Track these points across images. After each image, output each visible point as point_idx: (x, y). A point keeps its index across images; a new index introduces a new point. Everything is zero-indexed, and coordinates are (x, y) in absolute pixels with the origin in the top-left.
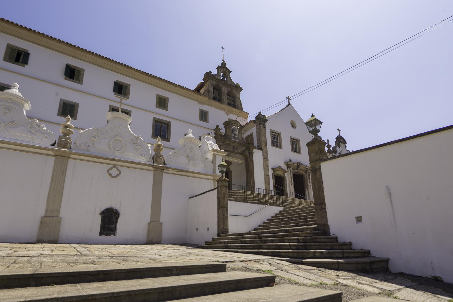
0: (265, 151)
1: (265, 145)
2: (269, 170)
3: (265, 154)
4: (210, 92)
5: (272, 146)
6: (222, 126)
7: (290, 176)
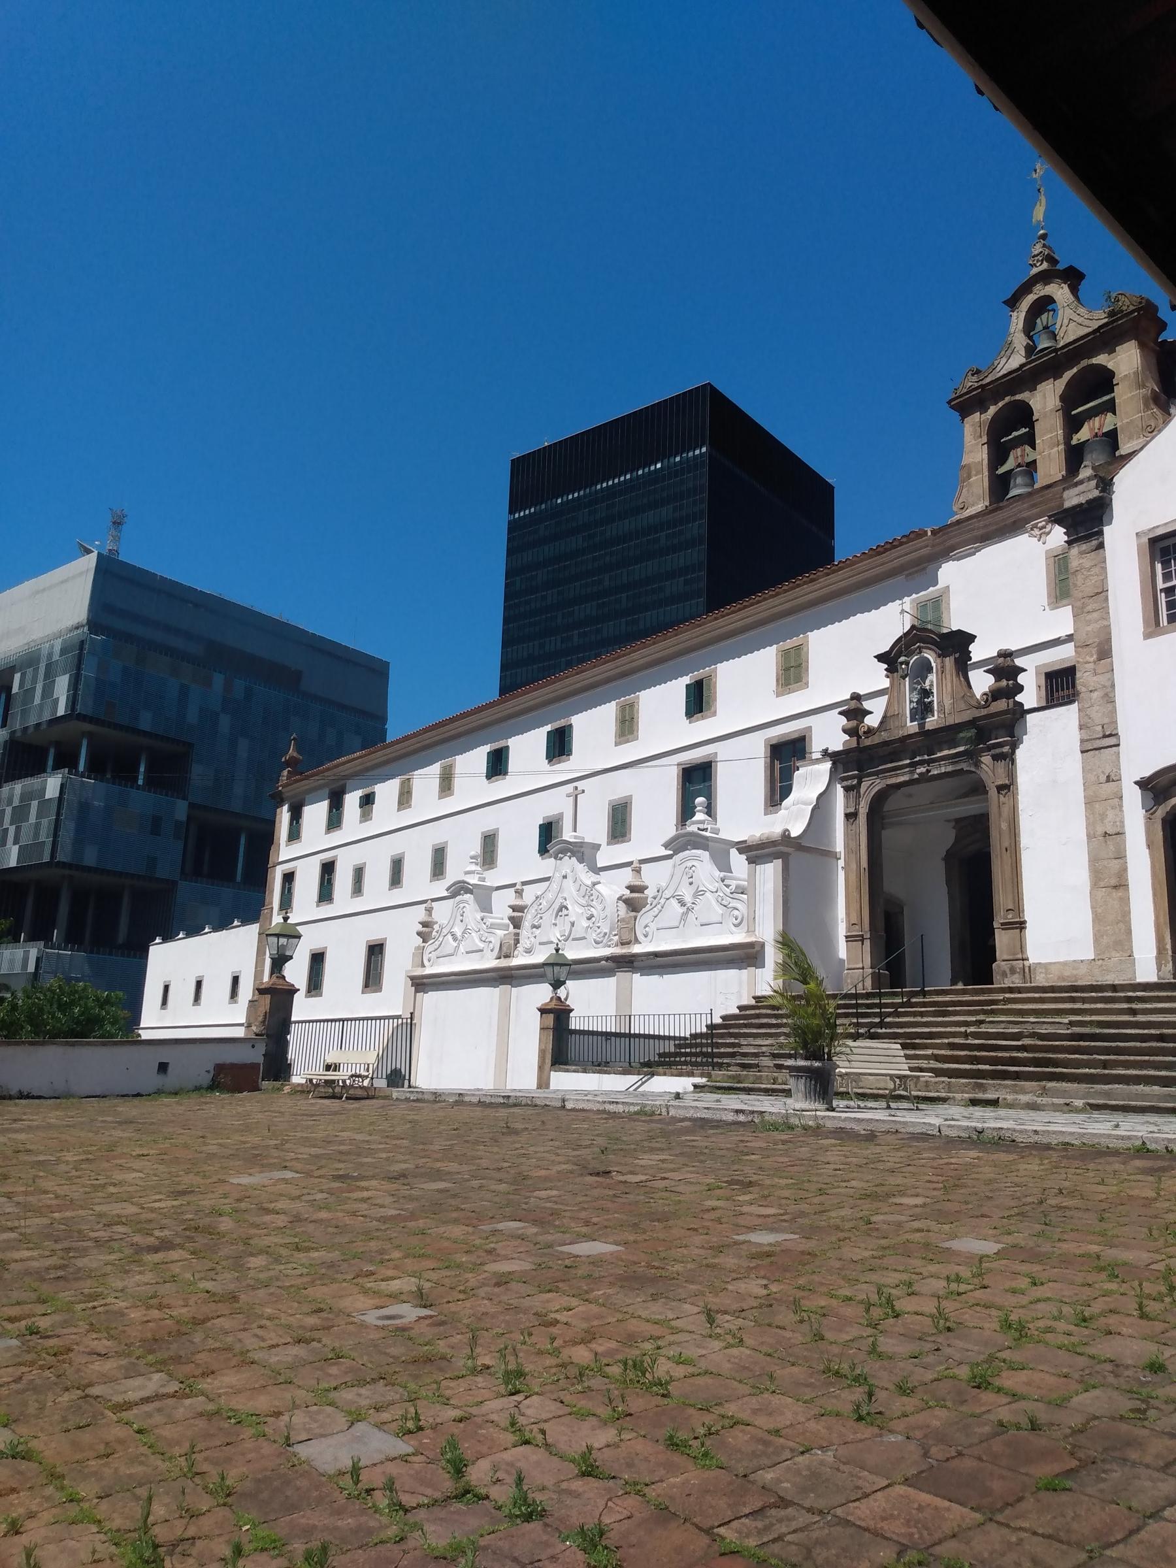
0: (1095, 695)
1: (1095, 657)
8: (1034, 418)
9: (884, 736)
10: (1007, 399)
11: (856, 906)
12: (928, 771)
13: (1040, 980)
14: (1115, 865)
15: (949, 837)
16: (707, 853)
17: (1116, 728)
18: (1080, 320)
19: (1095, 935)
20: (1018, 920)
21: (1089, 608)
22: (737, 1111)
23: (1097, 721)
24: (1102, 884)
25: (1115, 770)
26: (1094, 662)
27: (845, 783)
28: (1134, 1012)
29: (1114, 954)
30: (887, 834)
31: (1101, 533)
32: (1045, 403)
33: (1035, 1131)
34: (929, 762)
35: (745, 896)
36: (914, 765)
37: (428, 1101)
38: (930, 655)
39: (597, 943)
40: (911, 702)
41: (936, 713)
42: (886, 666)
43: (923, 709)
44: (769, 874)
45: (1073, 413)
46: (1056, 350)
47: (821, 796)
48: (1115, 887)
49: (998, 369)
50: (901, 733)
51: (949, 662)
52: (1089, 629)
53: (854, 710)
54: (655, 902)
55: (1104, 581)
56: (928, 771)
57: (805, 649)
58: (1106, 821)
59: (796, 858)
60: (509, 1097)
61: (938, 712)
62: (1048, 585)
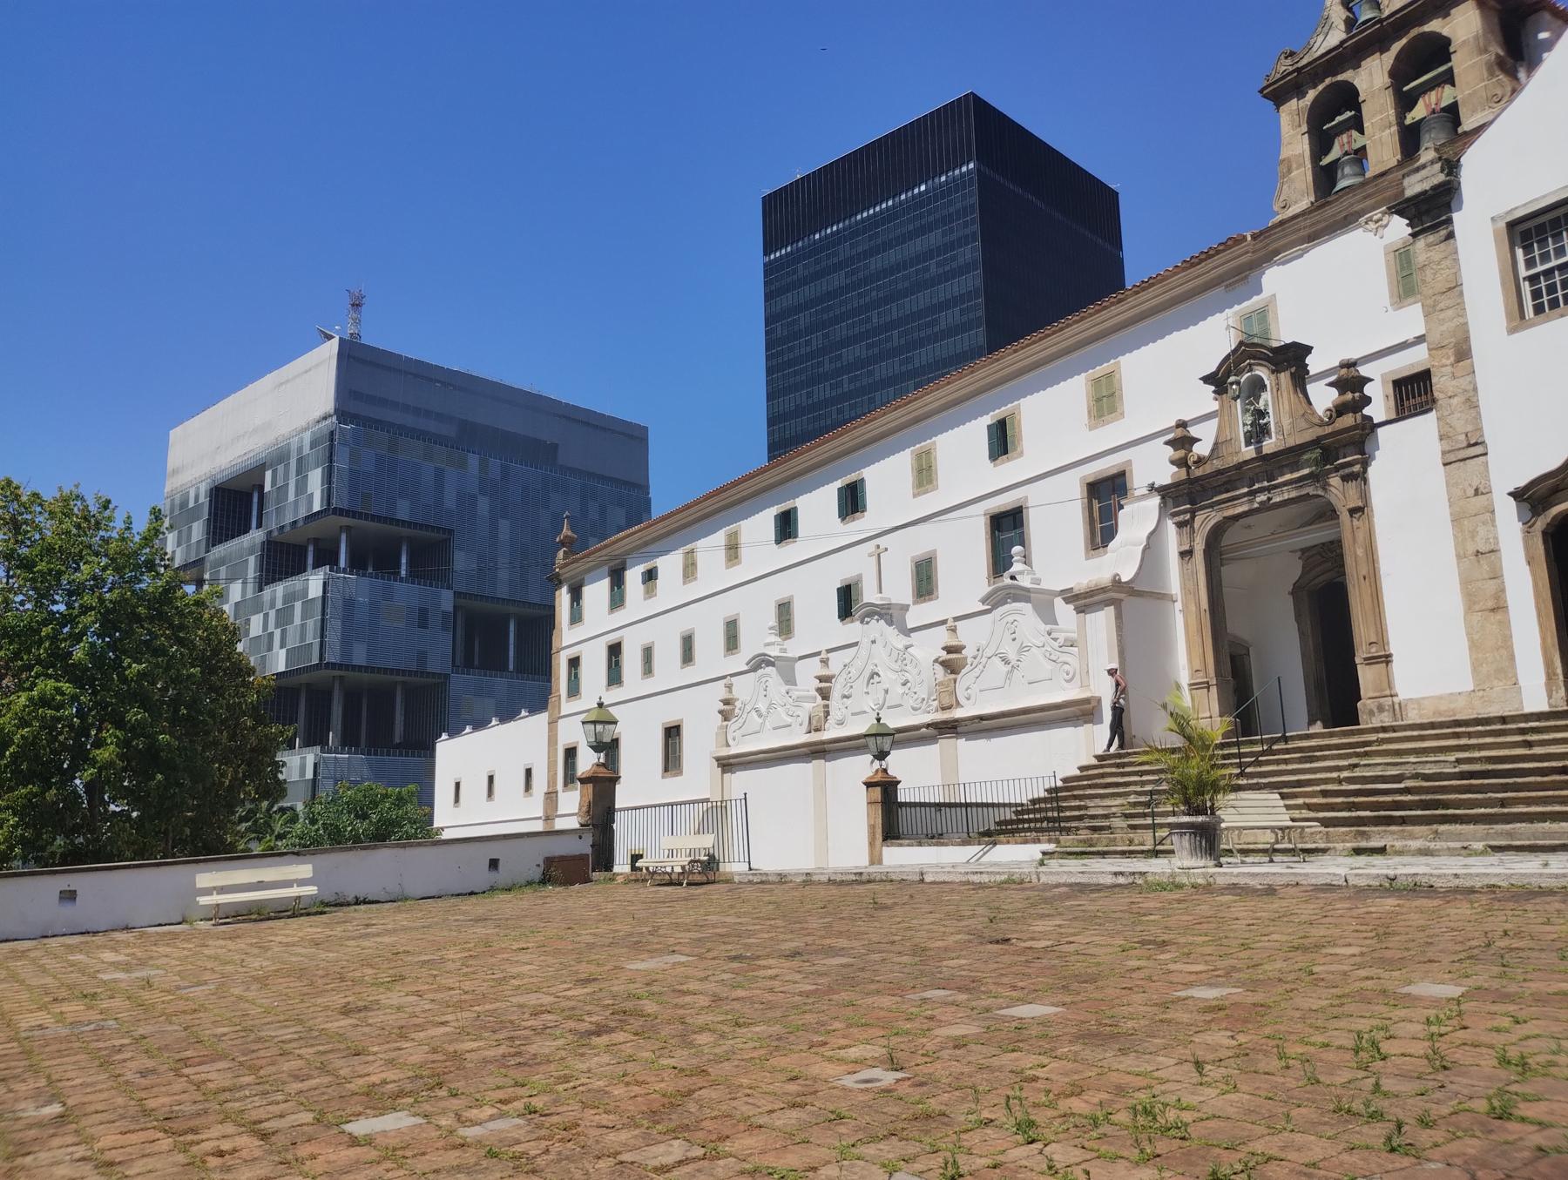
0: (1455, 401)
1: (1452, 359)
2: (1493, 512)
8: (1361, 99)
9: (1217, 464)
10: (1328, 81)
11: (1198, 650)
12: (1269, 499)
13: (1413, 717)
14: (1491, 586)
15: (1295, 570)
16: (1029, 605)
17: (1482, 436)
19: (1473, 664)
20: (1383, 653)
21: (1442, 306)
22: (1116, 874)
23: (1459, 430)
24: (1477, 607)
25: (1483, 482)
26: (1452, 365)
27: (1177, 519)
28: (1529, 744)
29: (1495, 683)
30: (1228, 573)
31: (1449, 221)
32: (1372, 82)
33: (1456, 875)
34: (1268, 489)
35: (1076, 649)
36: (1253, 493)
37: (774, 883)
38: (1262, 372)
39: (915, 709)
40: (1244, 425)
41: (1273, 435)
42: (1213, 388)
43: (1258, 432)
44: (1102, 621)
45: (1405, 89)
46: (1381, 21)
47: (1152, 533)
48: (1493, 610)
49: (1314, 49)
50: (1235, 459)
51: (1285, 377)
52: (1444, 328)
53: (1182, 441)
54: (976, 662)
55: (1457, 274)
56: (1269, 499)
57: (1117, 376)
58: (1478, 539)
59: (1130, 603)
60: (861, 874)
61: (1276, 433)
62: (1390, 283)
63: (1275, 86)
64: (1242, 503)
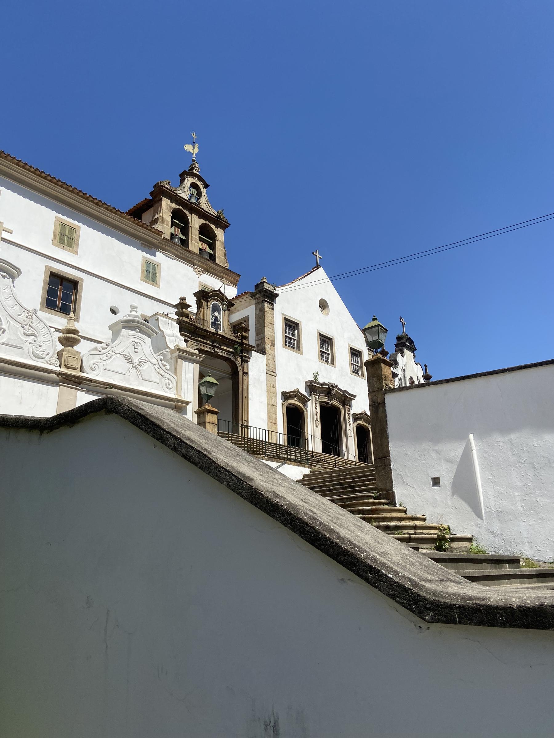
0: (270, 356)
3: (270, 361)
4: (165, 223)
5: (283, 347)
6: (192, 301)
7: (314, 409)
18: (208, 207)
21: (269, 326)
41: (222, 330)
52: (269, 333)
63: (168, 190)
64: (208, 348)
